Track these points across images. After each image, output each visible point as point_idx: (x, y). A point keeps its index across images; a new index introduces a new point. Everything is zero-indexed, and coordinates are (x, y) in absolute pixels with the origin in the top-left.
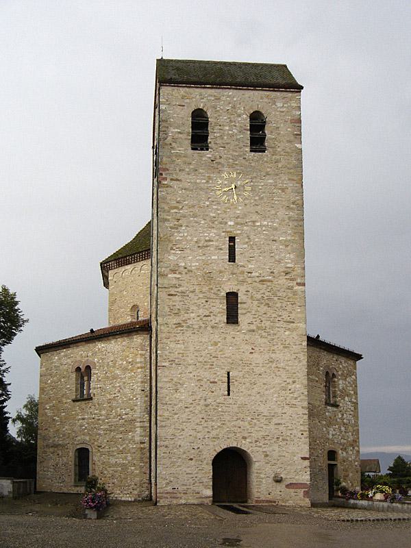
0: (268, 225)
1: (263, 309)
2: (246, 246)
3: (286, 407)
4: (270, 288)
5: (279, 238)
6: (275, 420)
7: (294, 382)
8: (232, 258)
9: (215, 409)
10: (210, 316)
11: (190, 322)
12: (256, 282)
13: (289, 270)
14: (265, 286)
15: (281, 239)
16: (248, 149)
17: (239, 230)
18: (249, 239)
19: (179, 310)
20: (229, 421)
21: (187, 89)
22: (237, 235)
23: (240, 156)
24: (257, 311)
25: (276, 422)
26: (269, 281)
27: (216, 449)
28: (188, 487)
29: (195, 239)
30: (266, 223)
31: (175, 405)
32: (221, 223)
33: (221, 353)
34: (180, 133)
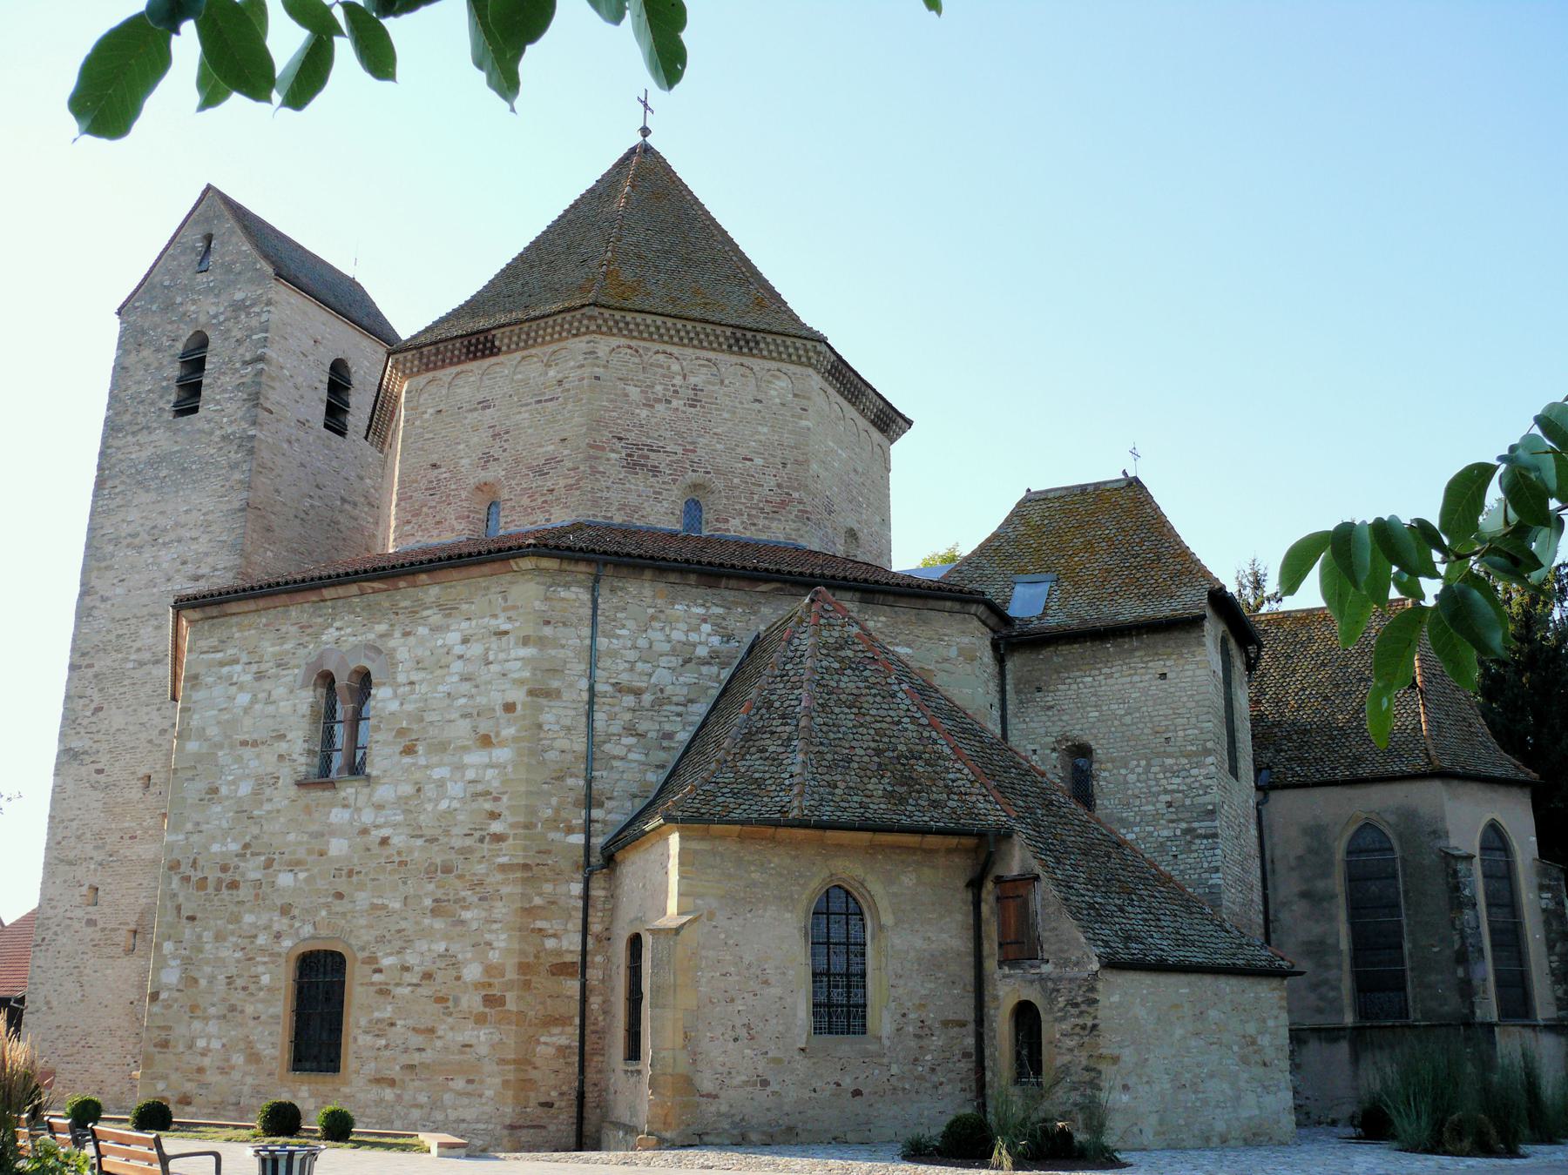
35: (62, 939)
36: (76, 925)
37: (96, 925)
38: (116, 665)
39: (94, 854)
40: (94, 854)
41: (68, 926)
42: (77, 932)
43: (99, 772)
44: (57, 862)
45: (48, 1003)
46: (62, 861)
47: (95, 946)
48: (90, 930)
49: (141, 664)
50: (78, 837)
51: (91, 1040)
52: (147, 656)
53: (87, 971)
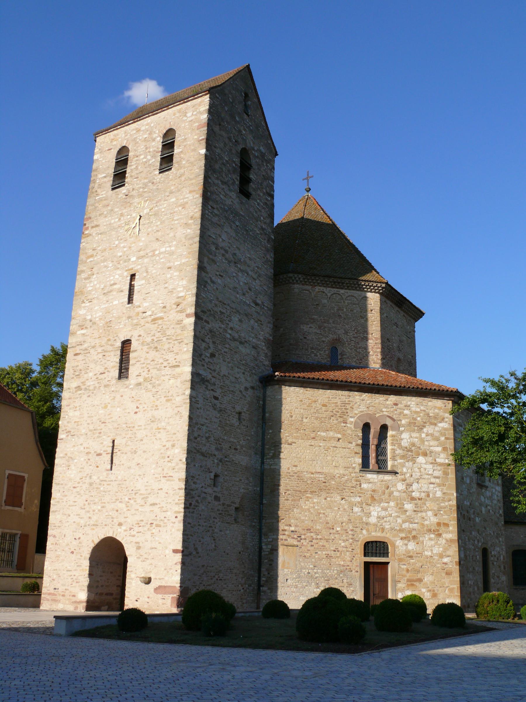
0: (166, 251)
1: (153, 354)
2: (143, 282)
3: (163, 480)
4: (160, 327)
6: (151, 499)
7: (173, 446)
8: (130, 300)
9: (97, 488)
10: (104, 373)
11: (88, 383)
12: (148, 322)
13: (180, 300)
14: (156, 325)
15: (176, 263)
16: (157, 172)
17: (139, 264)
18: (147, 272)
19: (81, 370)
20: (108, 503)
21: (115, 132)
22: (138, 271)
24: (146, 359)
25: (152, 502)
26: (162, 318)
27: (95, 540)
28: (67, 588)
29: (102, 286)
30: (163, 250)
31: (66, 485)
32: (125, 262)
33: (109, 417)
34: (105, 177)
35: (202, 507)
36: (209, 499)
37: (219, 501)
38: (221, 331)
39: (216, 453)
40: (216, 453)
41: (204, 498)
42: (209, 503)
43: (216, 398)
44: (196, 451)
45: (196, 549)
46: (198, 451)
47: (220, 514)
48: (217, 503)
49: (234, 339)
50: (207, 438)
51: (221, 575)
52: (236, 336)
53: (216, 530)
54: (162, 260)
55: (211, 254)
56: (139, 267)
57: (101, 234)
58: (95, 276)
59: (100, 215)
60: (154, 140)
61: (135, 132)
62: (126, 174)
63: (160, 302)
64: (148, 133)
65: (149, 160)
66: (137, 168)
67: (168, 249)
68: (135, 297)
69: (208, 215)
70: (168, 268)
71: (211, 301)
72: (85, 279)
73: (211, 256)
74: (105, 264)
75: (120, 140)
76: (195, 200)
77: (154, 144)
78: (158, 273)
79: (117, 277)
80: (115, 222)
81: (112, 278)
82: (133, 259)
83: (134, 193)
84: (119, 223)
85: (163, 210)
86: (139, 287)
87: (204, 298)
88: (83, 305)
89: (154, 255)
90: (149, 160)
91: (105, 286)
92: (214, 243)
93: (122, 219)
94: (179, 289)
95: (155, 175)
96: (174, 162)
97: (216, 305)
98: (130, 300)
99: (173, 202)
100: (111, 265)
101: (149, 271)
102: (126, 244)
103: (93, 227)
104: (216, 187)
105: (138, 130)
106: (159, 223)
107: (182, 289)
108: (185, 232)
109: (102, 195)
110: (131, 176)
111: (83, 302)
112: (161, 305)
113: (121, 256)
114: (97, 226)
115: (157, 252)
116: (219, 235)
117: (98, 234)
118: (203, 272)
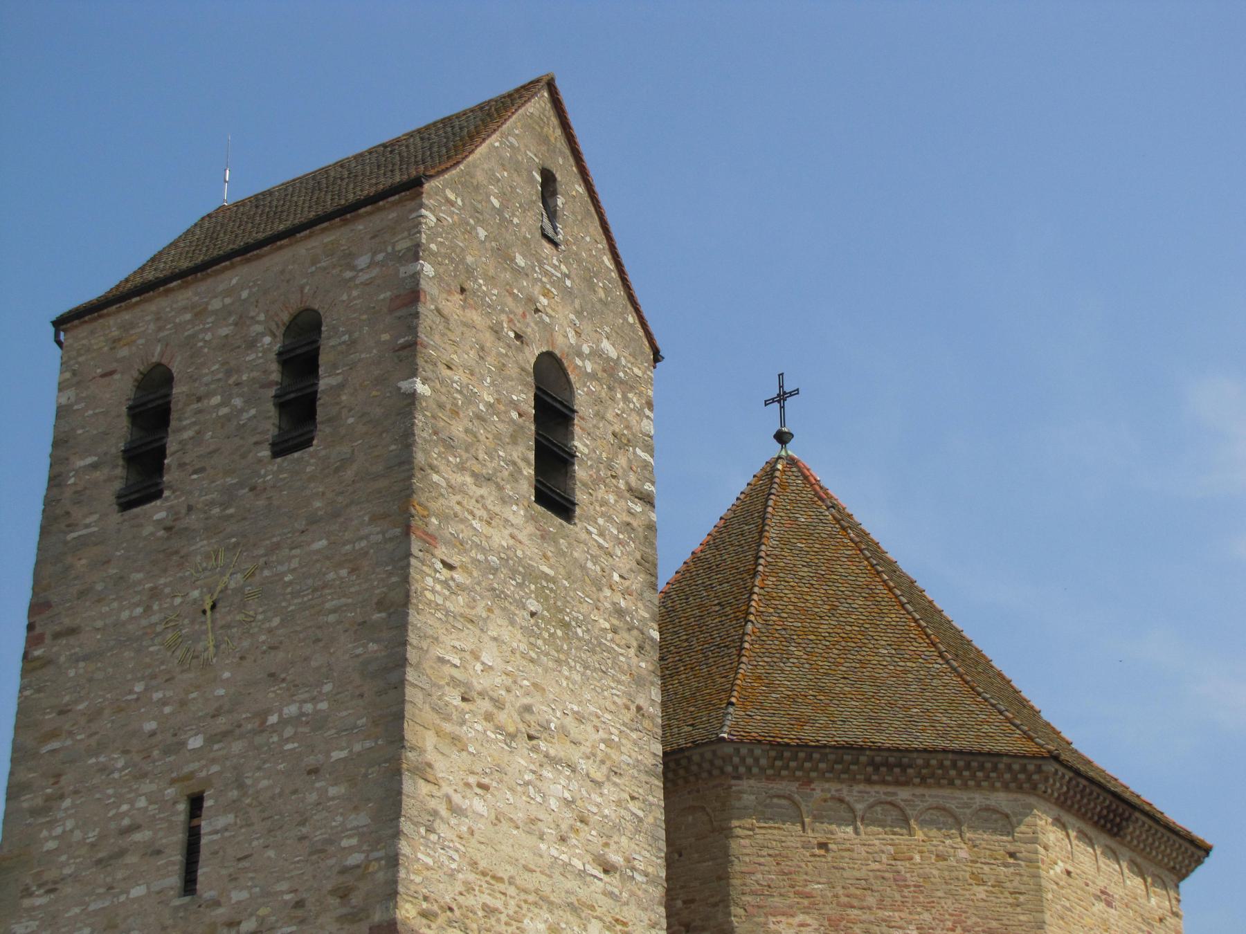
2: (230, 818)
5: (328, 753)
8: (189, 883)
15: (337, 755)
16: (265, 453)
17: (214, 761)
18: (241, 786)
22: (208, 781)
23: (241, 485)
29: (92, 836)
30: (291, 710)
32: (167, 751)
34: (94, 466)
54: (289, 746)
55: (447, 718)
56: (215, 768)
57: (86, 658)
58: (67, 803)
59: (82, 594)
60: (252, 344)
61: (188, 316)
62: (164, 457)
63: (284, 886)
64: (231, 320)
65: (242, 411)
66: (198, 439)
67: (308, 708)
68: (202, 872)
69: (433, 591)
70: (309, 773)
71: (452, 875)
72: (35, 812)
73: (448, 727)
74: (102, 759)
75: (142, 341)
76: (390, 546)
77: (253, 356)
78: (277, 791)
79: (142, 803)
80: (132, 619)
81: (125, 807)
82: (195, 742)
83: (193, 520)
84: (144, 622)
85: (288, 578)
86: (215, 837)
87: (428, 868)
88: (27, 903)
89: (262, 729)
90: (242, 411)
91: (102, 837)
92: (454, 682)
93: (156, 607)
94: (345, 843)
95: (260, 461)
96: (319, 418)
97: (469, 888)
98: (189, 883)
99: (318, 551)
100: (120, 764)
101: (248, 782)
102: (169, 693)
103: (57, 636)
104: (458, 498)
105: (200, 313)
106: (276, 621)
107: (354, 841)
108: (360, 651)
109: (87, 526)
110: (182, 466)
111: (27, 893)
112: (287, 897)
113: (153, 734)
114: (72, 631)
115: (273, 719)
116: (472, 652)
117: (76, 659)
118: (421, 783)
